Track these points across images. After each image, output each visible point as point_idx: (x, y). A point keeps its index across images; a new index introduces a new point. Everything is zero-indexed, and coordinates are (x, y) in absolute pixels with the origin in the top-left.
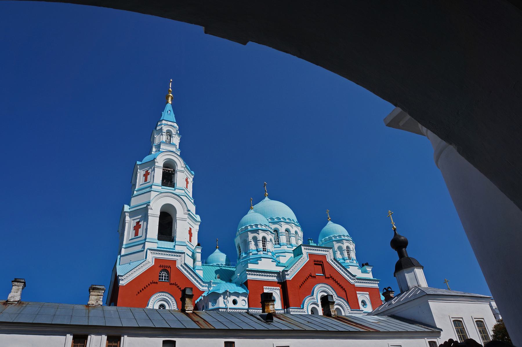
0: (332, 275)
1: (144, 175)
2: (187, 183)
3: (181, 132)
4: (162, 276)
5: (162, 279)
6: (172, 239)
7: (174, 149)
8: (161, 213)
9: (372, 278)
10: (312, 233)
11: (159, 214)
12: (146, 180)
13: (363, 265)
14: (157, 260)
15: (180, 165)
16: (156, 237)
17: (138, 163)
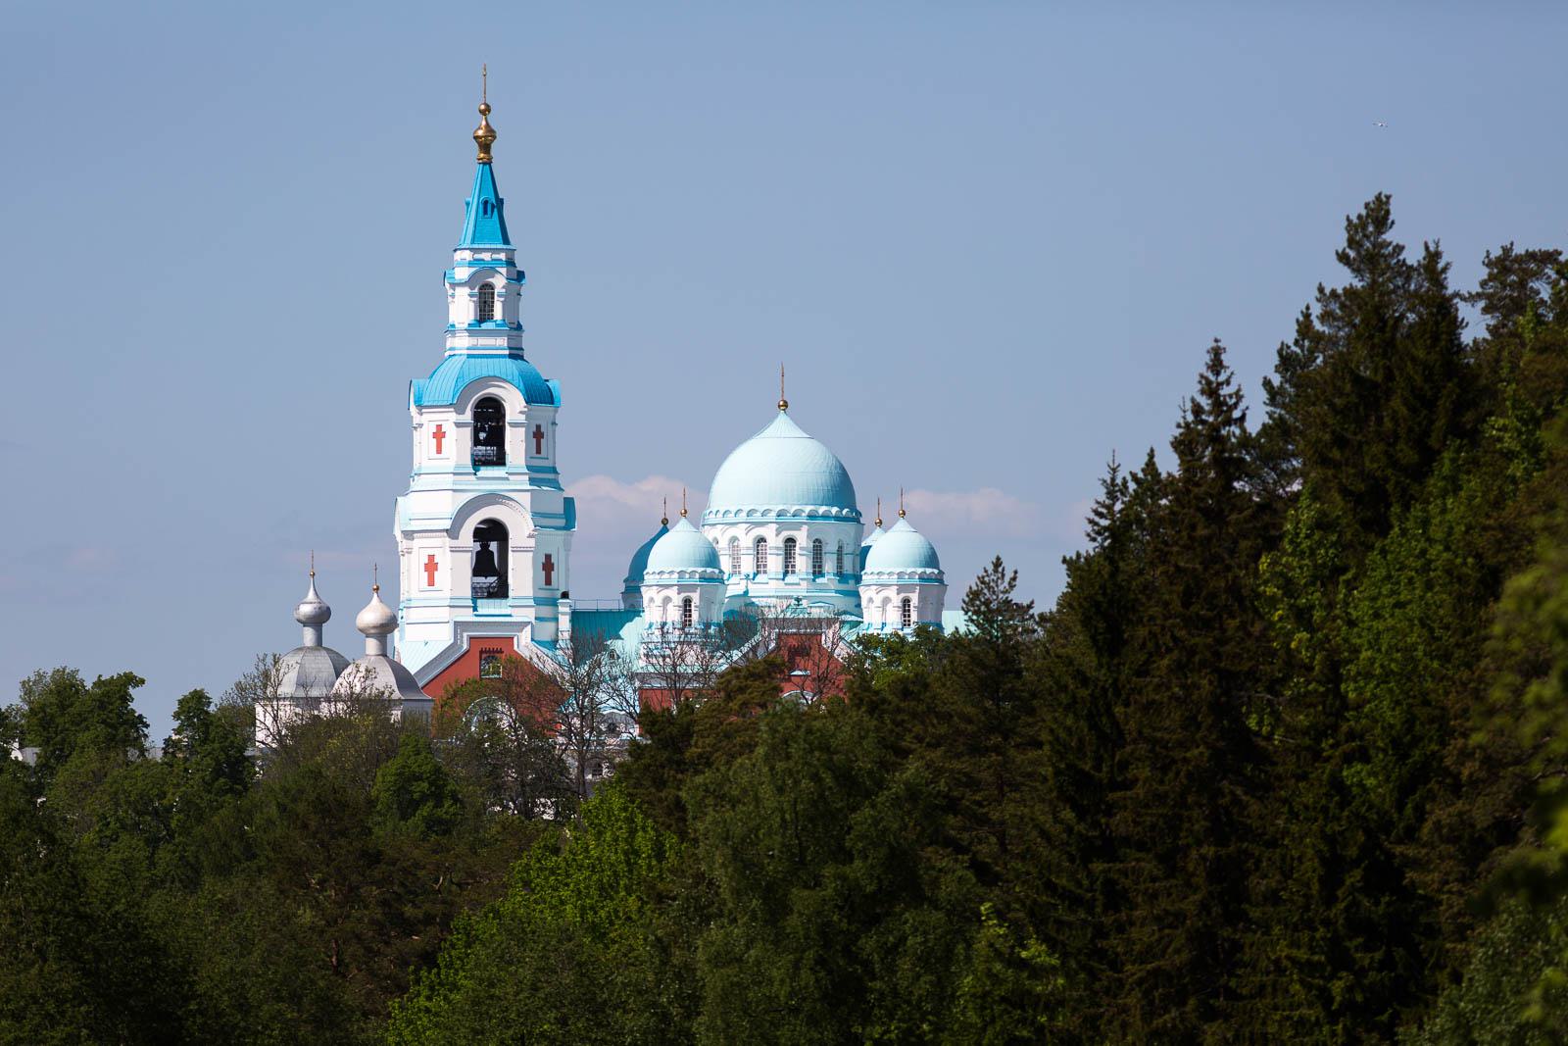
1: (435, 435)
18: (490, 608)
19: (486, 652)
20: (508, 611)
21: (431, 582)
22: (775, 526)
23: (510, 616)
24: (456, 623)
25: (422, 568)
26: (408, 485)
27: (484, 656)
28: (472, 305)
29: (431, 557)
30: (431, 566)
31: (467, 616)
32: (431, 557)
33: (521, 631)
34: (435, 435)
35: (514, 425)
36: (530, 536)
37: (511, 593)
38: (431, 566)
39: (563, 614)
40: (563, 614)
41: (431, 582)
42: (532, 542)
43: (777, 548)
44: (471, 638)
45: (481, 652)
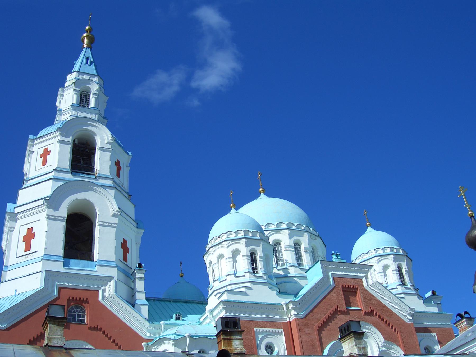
2: (119, 168)
3: (106, 87)
4: (74, 316)
11: (67, 216)
17: (31, 137)
21: (28, 248)
22: (287, 232)
24: (48, 272)
25: (21, 239)
26: (22, 174)
28: (75, 96)
31: (59, 267)
35: (102, 149)
36: (114, 215)
37: (96, 257)
39: (140, 279)
40: (140, 279)
41: (28, 248)
42: (116, 220)
43: (290, 247)
44: (60, 289)
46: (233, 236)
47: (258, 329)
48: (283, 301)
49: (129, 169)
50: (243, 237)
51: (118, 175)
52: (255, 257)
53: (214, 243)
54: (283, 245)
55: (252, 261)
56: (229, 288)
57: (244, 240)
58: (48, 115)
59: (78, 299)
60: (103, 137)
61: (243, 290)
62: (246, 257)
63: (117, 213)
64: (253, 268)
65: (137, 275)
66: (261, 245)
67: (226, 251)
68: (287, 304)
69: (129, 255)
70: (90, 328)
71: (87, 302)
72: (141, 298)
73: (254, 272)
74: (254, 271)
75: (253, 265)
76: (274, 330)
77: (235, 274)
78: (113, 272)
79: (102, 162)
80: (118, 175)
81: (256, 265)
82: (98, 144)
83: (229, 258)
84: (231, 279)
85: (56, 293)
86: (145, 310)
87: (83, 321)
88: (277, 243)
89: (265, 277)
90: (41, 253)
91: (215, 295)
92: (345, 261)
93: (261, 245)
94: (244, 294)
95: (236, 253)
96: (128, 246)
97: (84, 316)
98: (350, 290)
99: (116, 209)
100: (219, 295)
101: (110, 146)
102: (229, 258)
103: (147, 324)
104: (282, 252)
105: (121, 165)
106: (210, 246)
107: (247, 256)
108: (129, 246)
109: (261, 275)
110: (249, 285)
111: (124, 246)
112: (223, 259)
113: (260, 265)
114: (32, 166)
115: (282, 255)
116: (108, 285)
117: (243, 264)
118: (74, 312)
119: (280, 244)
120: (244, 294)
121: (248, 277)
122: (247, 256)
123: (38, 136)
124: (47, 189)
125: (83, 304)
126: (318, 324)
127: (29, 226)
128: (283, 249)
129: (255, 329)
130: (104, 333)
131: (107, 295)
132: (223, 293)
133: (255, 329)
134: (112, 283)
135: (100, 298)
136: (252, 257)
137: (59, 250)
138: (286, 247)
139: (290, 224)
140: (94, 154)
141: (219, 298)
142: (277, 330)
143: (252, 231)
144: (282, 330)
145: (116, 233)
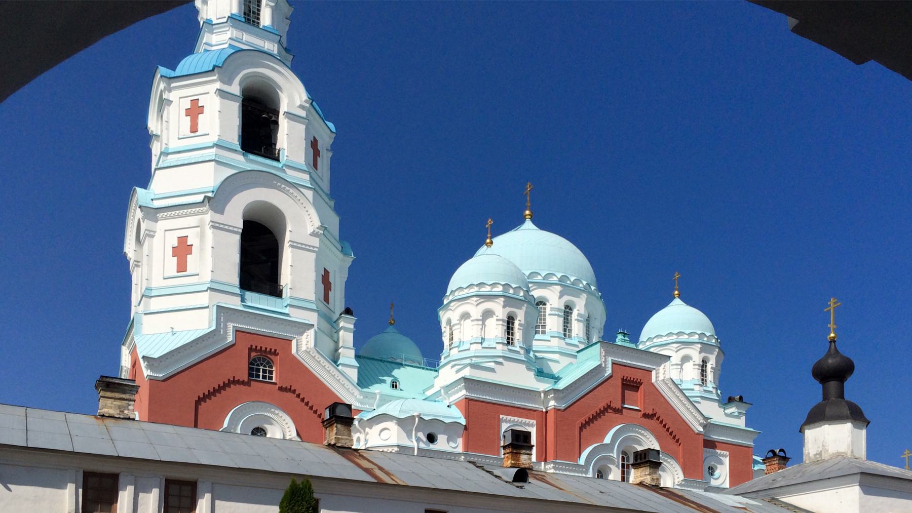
0: (657, 410)
1: (188, 112)
2: (316, 153)
4: (258, 370)
5: (258, 376)
6: (275, 291)
7: (271, 47)
8: (245, 222)
9: (743, 426)
10: (624, 308)
11: (240, 225)
12: (194, 129)
13: (731, 400)
14: (237, 331)
15: (292, 95)
16: (236, 281)
17: (162, 70)
18: (258, 301)
19: (256, 350)
20: (286, 311)
21: (182, 267)
23: (287, 315)
25: (169, 251)
27: (253, 354)
29: (183, 240)
30: (182, 250)
32: (183, 240)
33: (301, 334)
34: (188, 112)
36: (314, 234)
38: (182, 250)
39: (346, 330)
41: (182, 267)
42: (316, 242)
43: (559, 310)
45: (251, 350)
46: (486, 290)
47: (505, 417)
48: (543, 386)
49: (330, 154)
50: (501, 293)
51: (315, 165)
52: (513, 324)
53: (458, 294)
54: (548, 307)
55: (508, 328)
56: (475, 360)
57: (502, 299)
58: (189, 33)
59: (263, 349)
60: (292, 95)
61: (492, 365)
62: (501, 322)
63: (317, 230)
64: (508, 338)
65: (342, 324)
66: (524, 308)
67: (475, 309)
68: (546, 393)
69: (331, 294)
70: (281, 389)
71: (275, 354)
72: (348, 356)
73: (508, 343)
74: (509, 341)
75: (508, 334)
76: (524, 420)
77: (481, 343)
78: (312, 318)
79: (289, 138)
80: (315, 165)
81: (513, 335)
82: (283, 108)
83: (478, 320)
84: (476, 349)
85: (230, 338)
86: (353, 374)
87: (271, 378)
88: (542, 302)
89: (522, 352)
90: (207, 277)
91: (452, 367)
92: (633, 346)
93: (524, 308)
94: (492, 370)
95: (488, 314)
96: (331, 280)
97: (271, 372)
98: (631, 385)
99: (317, 223)
100: (458, 367)
101: (303, 114)
102: (478, 320)
103: (356, 393)
104: (545, 315)
105: (319, 147)
106: (451, 298)
107: (503, 320)
108: (331, 280)
109: (518, 349)
110: (501, 360)
111: (325, 280)
112: (468, 321)
113: (518, 335)
114: (167, 125)
115: (545, 320)
116: (305, 334)
117: (495, 330)
118: (258, 365)
119: (545, 304)
120: (492, 370)
121: (500, 350)
122: (503, 320)
123: (178, 73)
124: (207, 178)
125: (272, 357)
126: (582, 420)
127: (182, 233)
128: (548, 311)
129: (501, 416)
130: (298, 396)
131: (304, 348)
132: (465, 366)
133: (501, 416)
134: (311, 333)
135: (294, 351)
136: (508, 323)
137: (233, 277)
138: (552, 309)
139: (564, 278)
140: (276, 123)
141: (458, 371)
142: (528, 421)
143: (514, 286)
144: (535, 422)
145: (317, 259)
